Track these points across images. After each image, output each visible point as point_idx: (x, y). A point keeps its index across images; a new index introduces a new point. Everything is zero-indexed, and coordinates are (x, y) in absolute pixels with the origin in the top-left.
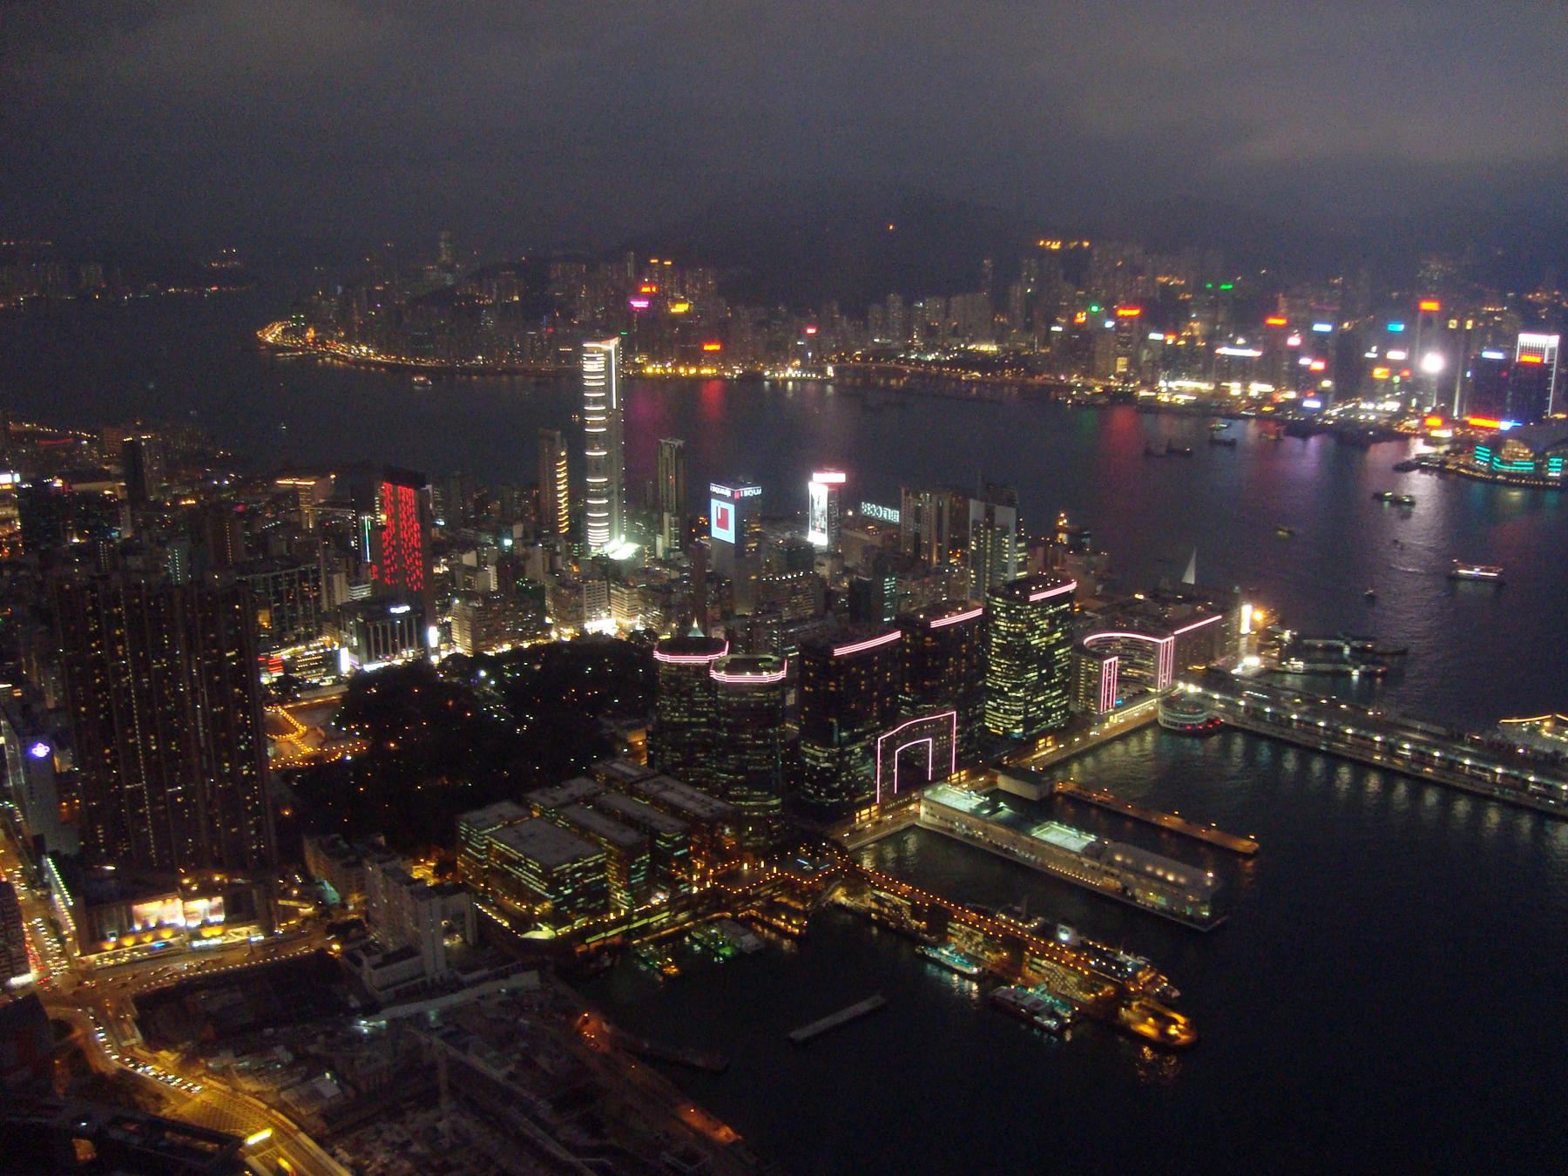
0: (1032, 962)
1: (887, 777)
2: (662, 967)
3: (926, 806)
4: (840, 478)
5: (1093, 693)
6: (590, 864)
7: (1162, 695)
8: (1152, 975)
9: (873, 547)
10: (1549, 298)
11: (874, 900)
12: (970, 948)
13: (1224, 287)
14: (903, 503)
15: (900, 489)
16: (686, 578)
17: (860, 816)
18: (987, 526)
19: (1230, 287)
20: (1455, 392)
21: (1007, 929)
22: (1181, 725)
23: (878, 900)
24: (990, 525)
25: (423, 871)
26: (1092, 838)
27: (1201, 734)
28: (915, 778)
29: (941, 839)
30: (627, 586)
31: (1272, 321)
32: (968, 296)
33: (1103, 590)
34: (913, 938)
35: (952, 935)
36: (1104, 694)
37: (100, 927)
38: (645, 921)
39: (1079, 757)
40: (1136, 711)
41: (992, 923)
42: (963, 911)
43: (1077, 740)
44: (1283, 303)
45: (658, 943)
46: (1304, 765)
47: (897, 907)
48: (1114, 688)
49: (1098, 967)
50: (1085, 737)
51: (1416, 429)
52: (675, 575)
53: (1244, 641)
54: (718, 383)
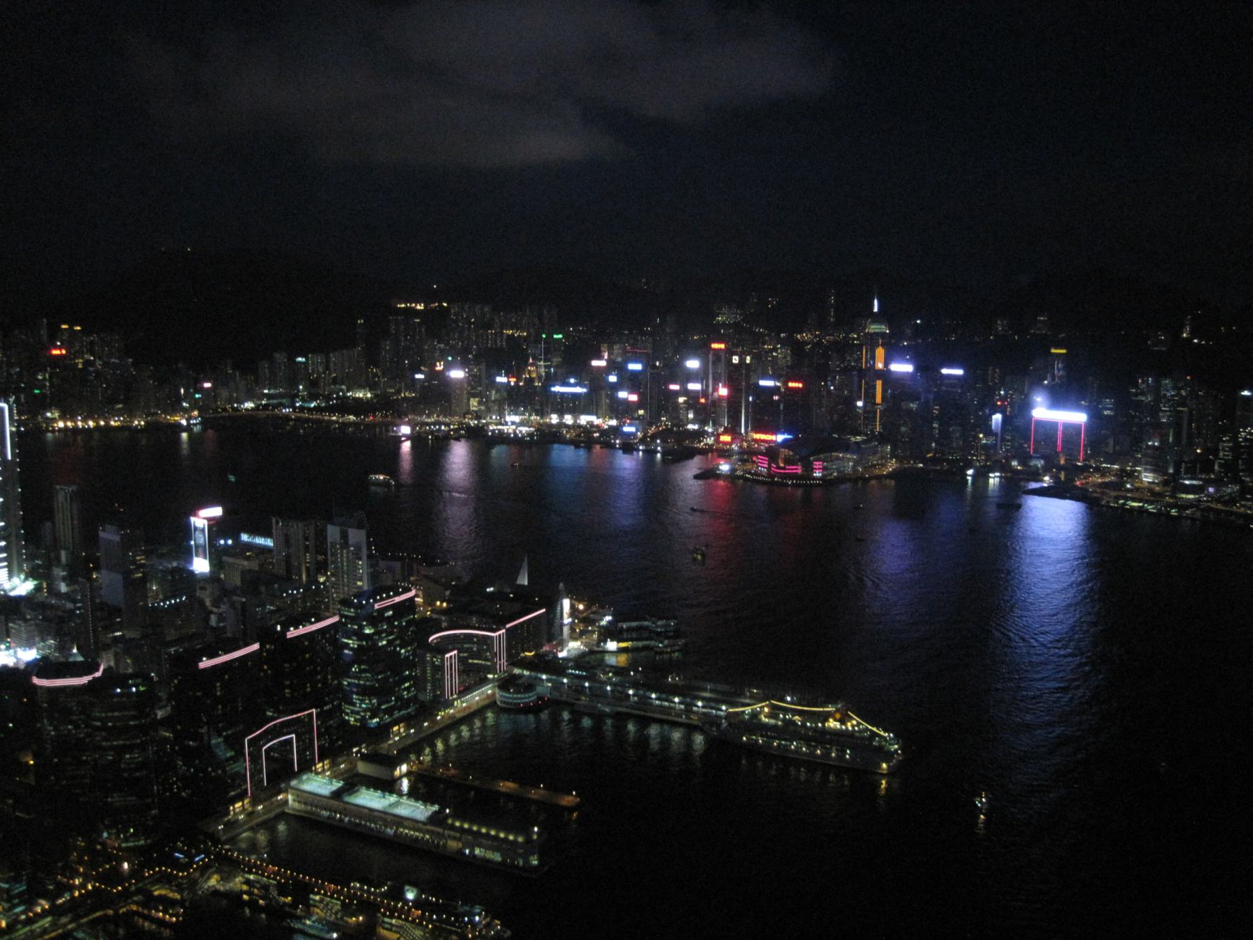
0: (384, 922)
1: (256, 772)
3: (293, 795)
4: (217, 511)
5: (439, 684)
7: (498, 680)
8: (488, 919)
9: (250, 571)
10: (812, 337)
12: (331, 916)
13: (555, 336)
14: (274, 531)
15: (272, 519)
16: (79, 608)
17: (234, 809)
18: (342, 548)
19: (560, 336)
20: (741, 412)
22: (515, 704)
23: (248, 882)
24: (345, 544)
26: (436, 808)
27: (532, 709)
28: (283, 772)
30: (25, 620)
31: (595, 363)
32: (344, 351)
33: (450, 594)
35: (315, 906)
36: (447, 684)
39: (430, 740)
40: (476, 697)
43: (426, 724)
44: (604, 347)
46: (620, 728)
47: (265, 888)
48: (456, 680)
49: (440, 920)
50: (434, 722)
51: (713, 445)
52: (70, 606)
53: (566, 630)
54: (126, 433)
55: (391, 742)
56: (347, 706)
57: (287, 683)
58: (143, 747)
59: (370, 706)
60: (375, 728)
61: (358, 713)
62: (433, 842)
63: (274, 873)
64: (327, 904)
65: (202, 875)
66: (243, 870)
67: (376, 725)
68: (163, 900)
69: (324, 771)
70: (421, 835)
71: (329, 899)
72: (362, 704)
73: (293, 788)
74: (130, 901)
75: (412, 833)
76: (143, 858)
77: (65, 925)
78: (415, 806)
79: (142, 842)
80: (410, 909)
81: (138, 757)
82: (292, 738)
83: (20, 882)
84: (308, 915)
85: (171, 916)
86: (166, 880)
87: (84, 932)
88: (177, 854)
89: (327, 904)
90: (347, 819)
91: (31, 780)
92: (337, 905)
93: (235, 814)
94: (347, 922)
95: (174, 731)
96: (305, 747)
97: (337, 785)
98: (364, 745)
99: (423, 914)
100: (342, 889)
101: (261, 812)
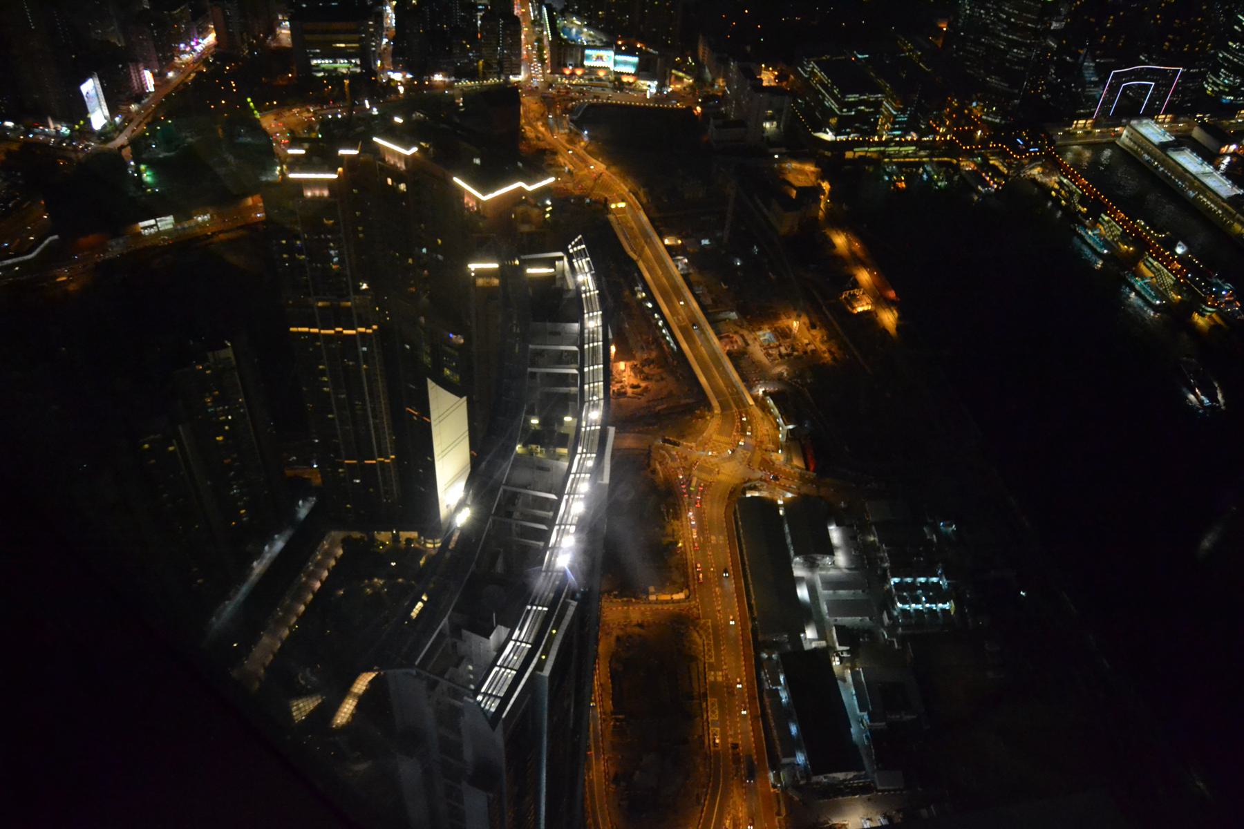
1: (1107, 102)
2: (895, 181)
3: (1128, 131)
6: (871, 99)
8: (1232, 298)
11: (1058, 183)
12: (1109, 236)
17: (1077, 123)
21: (1141, 232)
23: (1061, 183)
25: (768, 77)
28: (1130, 110)
29: (1127, 157)
34: (1071, 214)
37: (564, 59)
38: (897, 148)
41: (1133, 224)
42: (1116, 210)
45: (899, 165)
47: (1071, 193)
49: (1192, 280)
55: (1233, 121)
56: (1211, 76)
57: (1170, 37)
58: (1029, 48)
59: (1232, 84)
60: (1226, 104)
61: (1217, 85)
62: (1222, 218)
63: (1083, 185)
64: (1112, 226)
65: (1030, 163)
66: (1061, 173)
67: (1228, 101)
68: (994, 168)
69: (1163, 122)
70: (1215, 208)
71: (1114, 223)
72: (1225, 79)
73: (1132, 127)
74: (971, 159)
75: (1209, 203)
76: (995, 132)
77: (922, 157)
78: (1224, 183)
79: (998, 121)
80: (1174, 259)
81: (1023, 54)
82: (1152, 85)
83: (904, 115)
84: (1093, 227)
85: (995, 183)
86: (1002, 155)
87: (932, 168)
88: (1019, 140)
89: (1112, 226)
90: (1161, 169)
91: (940, 43)
92: (1118, 231)
93: (1076, 128)
94: (1119, 247)
95: (1060, 44)
96: (1159, 95)
97: (1169, 138)
98: (1208, 115)
99: (1181, 269)
100: (1129, 221)
101: (1097, 134)
